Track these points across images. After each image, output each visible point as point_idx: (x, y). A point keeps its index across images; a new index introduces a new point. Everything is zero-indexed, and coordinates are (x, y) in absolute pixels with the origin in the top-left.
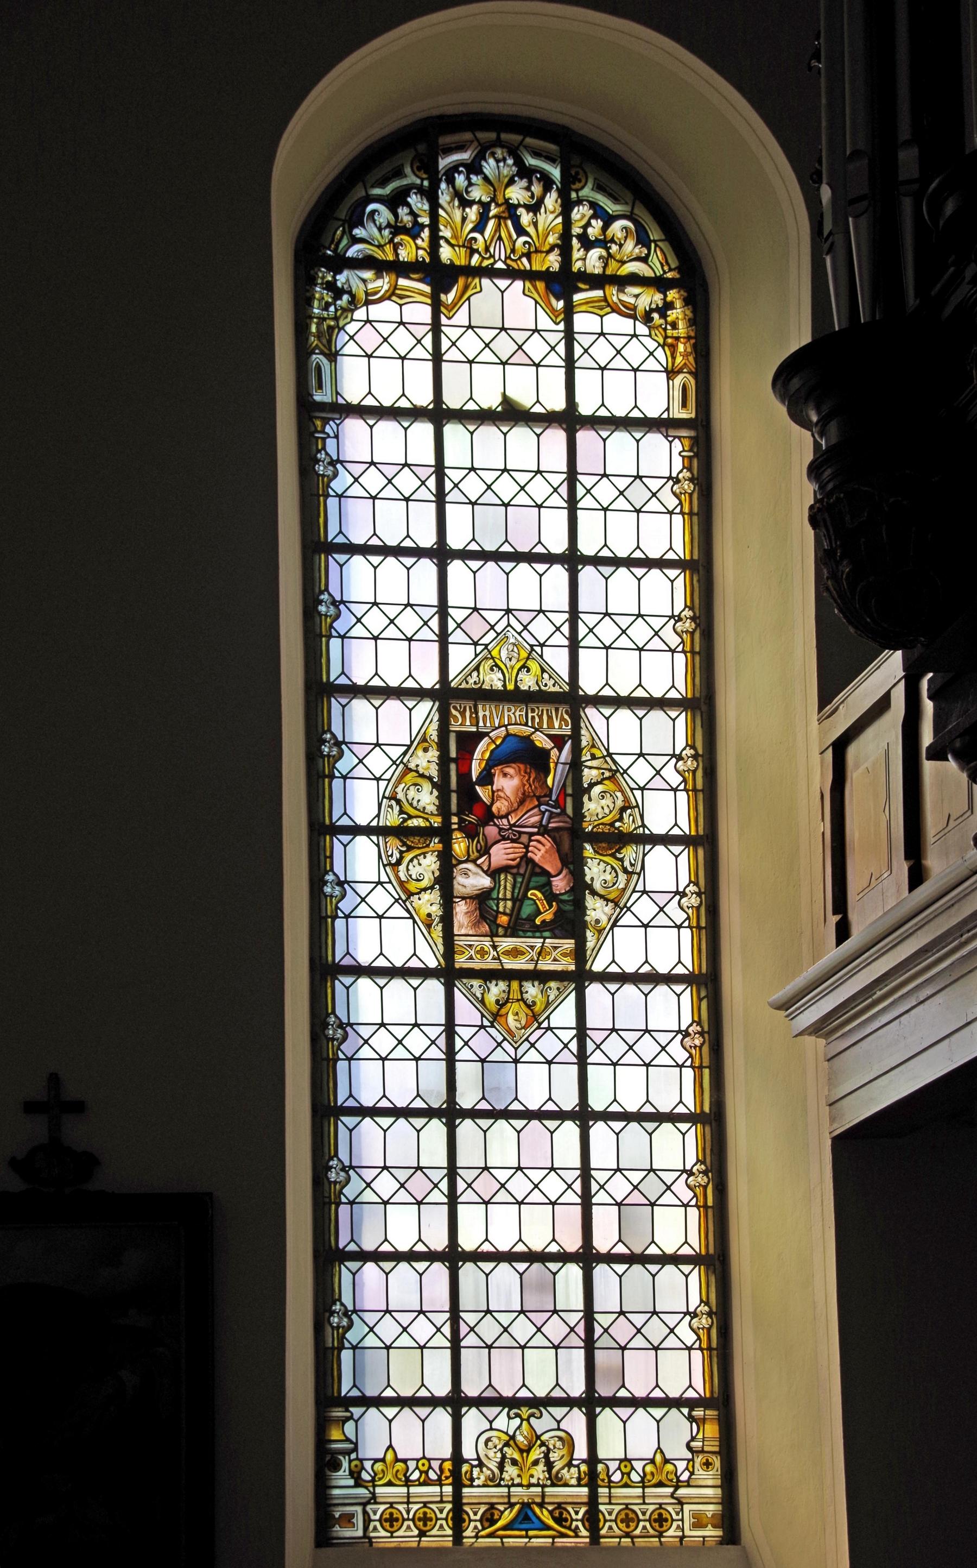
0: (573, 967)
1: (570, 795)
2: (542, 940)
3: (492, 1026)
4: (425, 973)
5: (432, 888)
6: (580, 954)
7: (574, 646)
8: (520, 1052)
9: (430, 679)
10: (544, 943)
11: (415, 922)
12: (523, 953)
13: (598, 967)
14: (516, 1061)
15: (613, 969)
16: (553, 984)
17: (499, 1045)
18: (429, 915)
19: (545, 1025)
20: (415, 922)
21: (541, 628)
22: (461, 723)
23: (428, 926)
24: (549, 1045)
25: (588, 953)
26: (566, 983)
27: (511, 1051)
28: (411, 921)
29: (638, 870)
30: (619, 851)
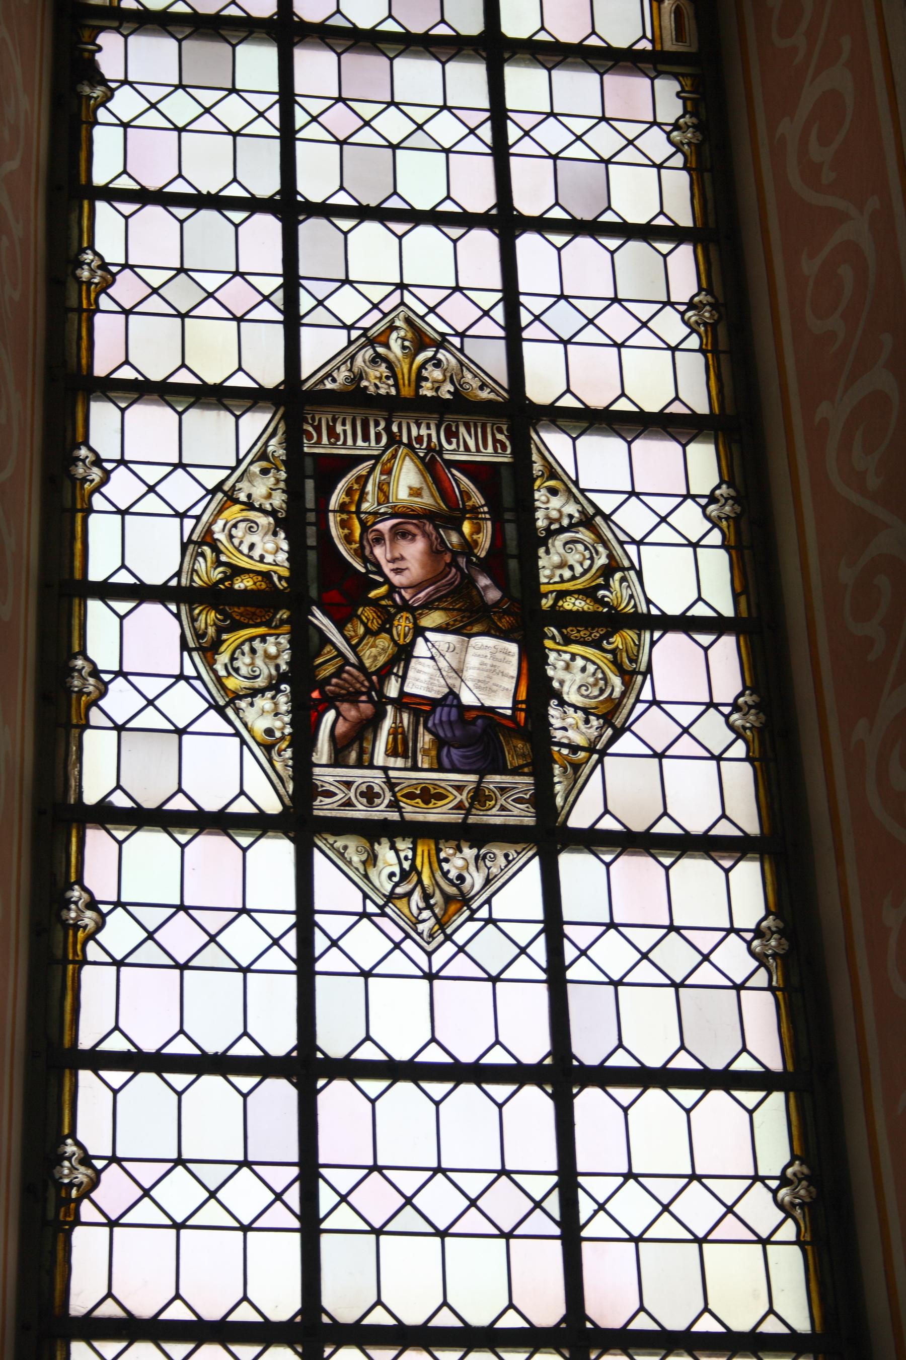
0: (530, 821)
1: (513, 557)
2: (473, 778)
3: (384, 914)
4: (260, 824)
5: (273, 687)
6: (542, 800)
8: (438, 959)
11: (243, 742)
12: (441, 797)
13: (579, 819)
15: (607, 823)
16: (498, 851)
17: (397, 946)
18: (269, 732)
19: (483, 913)
20: (243, 742)
21: (458, 312)
23: (268, 748)
24: (491, 949)
25: (559, 801)
26: (519, 847)
29: (643, 668)
30: (607, 636)
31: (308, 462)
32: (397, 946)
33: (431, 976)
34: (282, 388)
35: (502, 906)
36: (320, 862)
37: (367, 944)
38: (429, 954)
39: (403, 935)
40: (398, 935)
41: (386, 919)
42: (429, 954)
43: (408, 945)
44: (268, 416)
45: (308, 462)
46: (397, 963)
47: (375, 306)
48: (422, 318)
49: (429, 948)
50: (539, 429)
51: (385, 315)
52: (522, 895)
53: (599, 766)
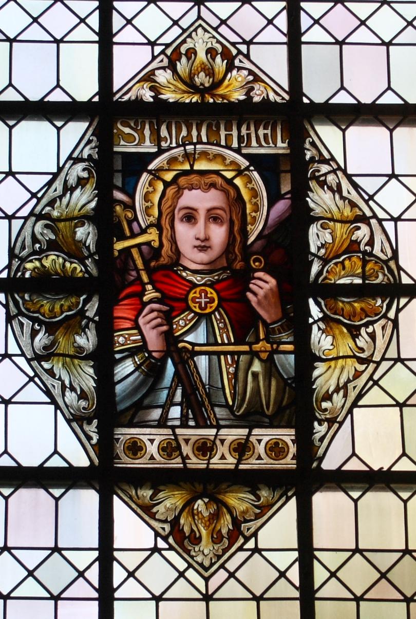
7: (294, 40)
8: (214, 583)
9: (85, 89)
10: (249, 434)
13: (329, 464)
14: (207, 598)
15: (354, 465)
22: (133, 141)
24: (257, 574)
27: (200, 583)
28: (52, 407)
31: (118, 165)
32: (182, 574)
33: (207, 598)
34: (96, 99)
35: (266, 538)
36: (119, 507)
37: (158, 573)
38: (207, 580)
39: (186, 565)
40: (182, 565)
41: (173, 553)
42: (207, 580)
43: (191, 574)
44: (87, 124)
45: (118, 165)
46: (181, 589)
47: (176, 23)
48: (216, 29)
49: (206, 574)
50: (314, 123)
51: (184, 31)
52: (281, 528)
53: (350, 416)
